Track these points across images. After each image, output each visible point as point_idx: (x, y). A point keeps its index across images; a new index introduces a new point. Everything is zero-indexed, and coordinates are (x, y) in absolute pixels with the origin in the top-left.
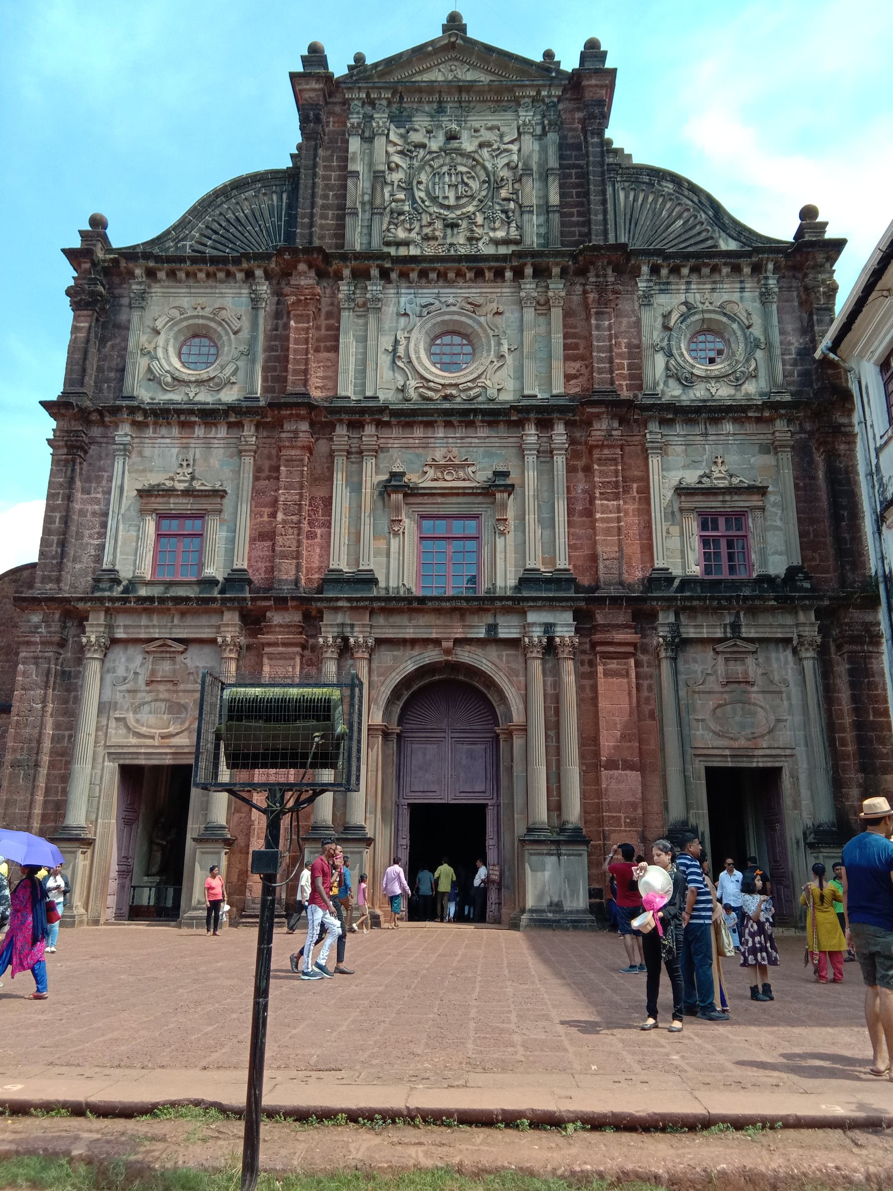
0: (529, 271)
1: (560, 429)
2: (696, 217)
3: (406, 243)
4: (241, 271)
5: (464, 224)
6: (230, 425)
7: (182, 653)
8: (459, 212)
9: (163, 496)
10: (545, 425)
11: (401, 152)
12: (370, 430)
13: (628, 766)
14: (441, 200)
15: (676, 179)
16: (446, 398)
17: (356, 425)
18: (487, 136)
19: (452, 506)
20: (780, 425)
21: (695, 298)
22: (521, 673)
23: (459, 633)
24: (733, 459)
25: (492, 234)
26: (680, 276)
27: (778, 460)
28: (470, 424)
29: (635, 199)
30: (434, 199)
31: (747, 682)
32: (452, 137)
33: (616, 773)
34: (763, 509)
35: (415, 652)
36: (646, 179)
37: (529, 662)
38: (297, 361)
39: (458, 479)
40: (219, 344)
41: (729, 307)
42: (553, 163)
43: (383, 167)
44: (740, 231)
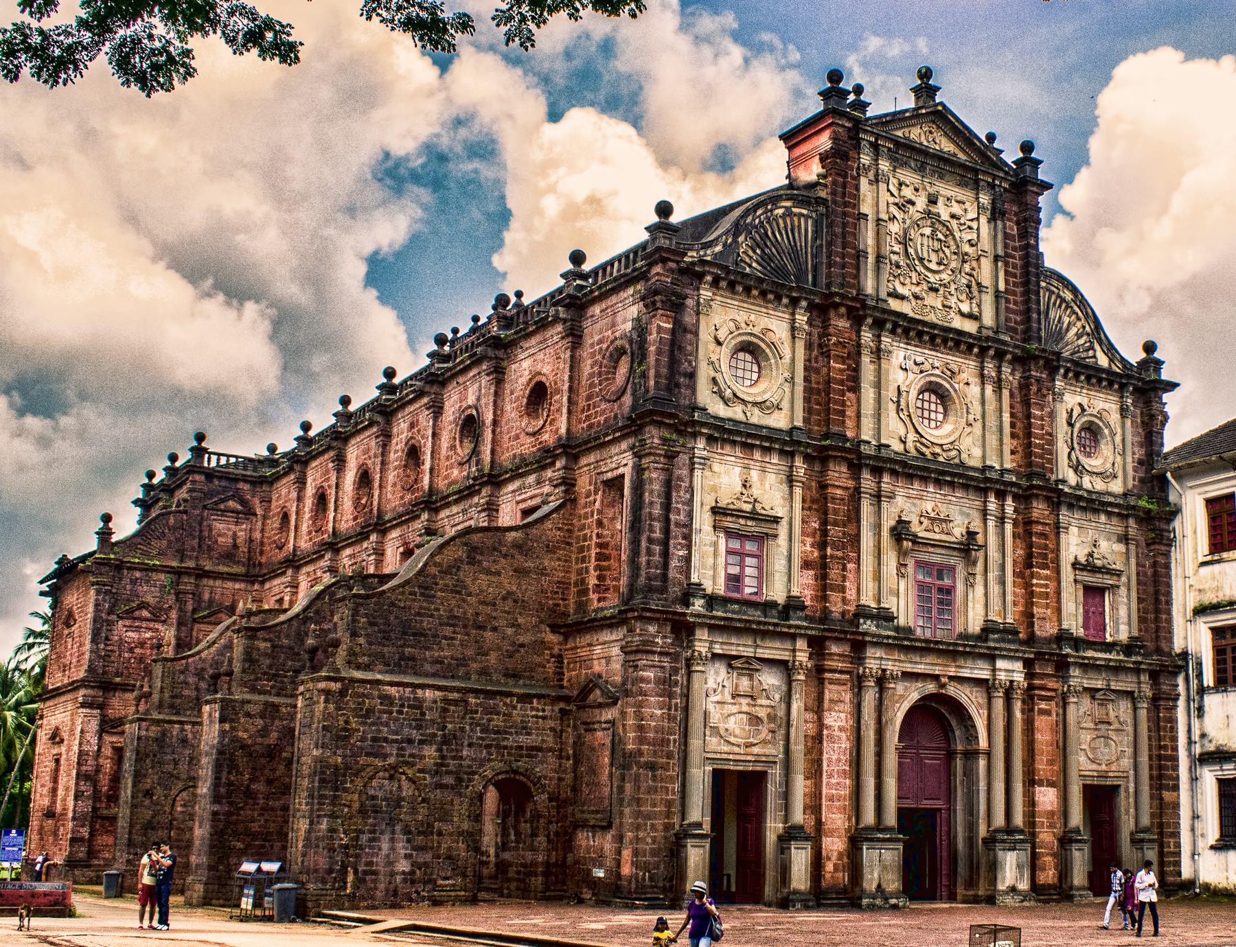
0: (992, 352)
2: (1084, 327)
4: (788, 296)
5: (942, 290)
6: (782, 452)
7: (757, 670)
8: (937, 277)
9: (732, 515)
10: (1001, 495)
11: (896, 204)
12: (886, 478)
13: (1051, 784)
14: (926, 262)
15: (1075, 291)
16: (933, 454)
17: (877, 472)
19: (936, 557)
20: (1131, 522)
21: (1085, 402)
22: (985, 706)
23: (952, 671)
24: (1104, 545)
25: (960, 304)
26: (1078, 380)
27: (1127, 549)
28: (952, 484)
30: (921, 260)
31: (1109, 723)
33: (1043, 789)
34: (1118, 587)
36: (1055, 283)
37: (994, 700)
38: (836, 402)
39: (942, 532)
41: (1104, 413)
43: (885, 217)
44: (1110, 350)
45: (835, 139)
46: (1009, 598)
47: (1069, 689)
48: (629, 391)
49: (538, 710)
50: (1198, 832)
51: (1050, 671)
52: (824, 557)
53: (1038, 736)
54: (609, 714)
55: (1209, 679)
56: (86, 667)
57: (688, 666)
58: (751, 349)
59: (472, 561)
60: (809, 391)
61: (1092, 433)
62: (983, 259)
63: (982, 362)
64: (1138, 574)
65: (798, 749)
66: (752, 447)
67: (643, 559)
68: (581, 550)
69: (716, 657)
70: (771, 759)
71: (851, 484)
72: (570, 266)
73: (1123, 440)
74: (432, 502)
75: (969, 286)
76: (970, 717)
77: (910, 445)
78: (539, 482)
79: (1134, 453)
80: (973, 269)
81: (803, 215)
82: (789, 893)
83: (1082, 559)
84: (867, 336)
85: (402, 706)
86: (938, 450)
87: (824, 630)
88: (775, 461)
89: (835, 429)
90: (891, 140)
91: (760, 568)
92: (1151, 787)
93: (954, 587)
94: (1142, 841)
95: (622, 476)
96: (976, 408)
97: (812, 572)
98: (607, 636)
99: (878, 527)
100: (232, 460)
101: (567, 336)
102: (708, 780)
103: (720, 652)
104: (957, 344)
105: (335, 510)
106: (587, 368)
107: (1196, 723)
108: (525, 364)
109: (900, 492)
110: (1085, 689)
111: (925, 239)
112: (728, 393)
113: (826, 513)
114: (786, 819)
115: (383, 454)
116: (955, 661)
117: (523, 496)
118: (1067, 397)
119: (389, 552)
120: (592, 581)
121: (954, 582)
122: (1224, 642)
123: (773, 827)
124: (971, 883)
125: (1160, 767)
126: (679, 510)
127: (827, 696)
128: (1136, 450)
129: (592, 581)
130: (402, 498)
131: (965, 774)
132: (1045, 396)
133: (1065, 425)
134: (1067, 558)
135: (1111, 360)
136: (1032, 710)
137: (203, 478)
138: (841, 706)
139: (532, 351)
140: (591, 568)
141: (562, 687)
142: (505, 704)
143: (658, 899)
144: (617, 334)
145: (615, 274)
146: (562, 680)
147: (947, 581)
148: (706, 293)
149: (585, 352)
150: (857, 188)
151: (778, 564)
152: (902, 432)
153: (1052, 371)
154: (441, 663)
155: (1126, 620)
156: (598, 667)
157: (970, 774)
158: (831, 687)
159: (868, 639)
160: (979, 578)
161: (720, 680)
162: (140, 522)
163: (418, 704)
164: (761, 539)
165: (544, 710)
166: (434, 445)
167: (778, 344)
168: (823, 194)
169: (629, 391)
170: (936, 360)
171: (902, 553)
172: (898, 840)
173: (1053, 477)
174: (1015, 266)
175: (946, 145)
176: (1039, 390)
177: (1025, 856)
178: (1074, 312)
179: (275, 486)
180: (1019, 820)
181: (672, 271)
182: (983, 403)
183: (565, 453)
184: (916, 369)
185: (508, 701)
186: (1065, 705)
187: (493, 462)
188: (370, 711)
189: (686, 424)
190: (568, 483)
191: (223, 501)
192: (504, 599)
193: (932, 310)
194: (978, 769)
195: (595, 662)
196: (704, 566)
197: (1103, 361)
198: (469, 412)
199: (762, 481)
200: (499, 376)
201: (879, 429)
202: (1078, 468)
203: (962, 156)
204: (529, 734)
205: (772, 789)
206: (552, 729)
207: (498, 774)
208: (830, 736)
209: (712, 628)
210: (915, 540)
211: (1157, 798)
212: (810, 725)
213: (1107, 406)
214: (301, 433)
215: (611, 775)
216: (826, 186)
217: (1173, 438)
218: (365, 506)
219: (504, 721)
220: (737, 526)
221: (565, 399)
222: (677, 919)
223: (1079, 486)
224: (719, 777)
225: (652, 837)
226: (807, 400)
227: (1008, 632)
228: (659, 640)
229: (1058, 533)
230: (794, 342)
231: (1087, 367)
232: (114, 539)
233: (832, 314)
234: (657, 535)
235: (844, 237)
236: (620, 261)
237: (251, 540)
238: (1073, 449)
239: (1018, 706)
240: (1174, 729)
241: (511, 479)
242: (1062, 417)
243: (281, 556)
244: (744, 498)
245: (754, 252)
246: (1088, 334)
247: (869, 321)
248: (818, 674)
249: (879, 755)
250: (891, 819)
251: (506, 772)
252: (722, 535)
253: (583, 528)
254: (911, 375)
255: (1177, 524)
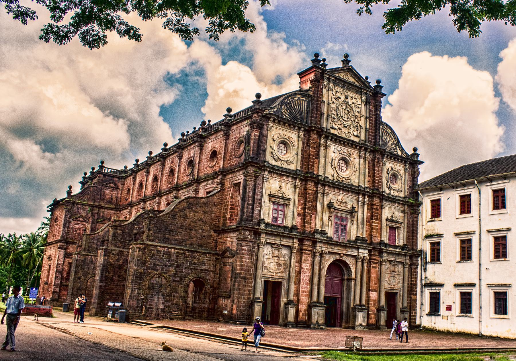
0: (363, 148)
1: (366, 197)
2: (394, 142)
3: (335, 129)
4: (297, 126)
5: (348, 128)
6: (293, 178)
7: (281, 248)
8: (347, 123)
9: (275, 197)
10: (364, 195)
11: (335, 98)
12: (326, 188)
13: (375, 291)
15: (391, 130)
16: (342, 181)
17: (324, 185)
18: (354, 101)
19: (341, 214)
20: (406, 206)
21: (393, 166)
22: (355, 264)
23: (345, 252)
26: (391, 159)
27: (404, 215)
28: (348, 191)
29: (383, 132)
30: (342, 117)
31: (395, 272)
32: (346, 98)
34: (400, 227)
35: (334, 256)
38: (311, 162)
39: (344, 206)
40: (288, 148)
42: (368, 116)
44: (402, 150)
45: (316, 76)
46: (365, 229)
47: (383, 260)
48: (244, 155)
49: (208, 258)
50: (423, 309)
51: (377, 254)
52: (305, 212)
53: (372, 275)
54: (232, 260)
55: (429, 259)
56: (61, 236)
57: (258, 246)
58: (284, 143)
59: (189, 208)
60: (303, 158)
61: (395, 177)
62: (362, 118)
63: (360, 151)
64: (407, 224)
65: (293, 275)
66: (283, 175)
67: (245, 210)
68: (225, 206)
69: (267, 243)
70: (284, 278)
71: (315, 189)
72: (227, 113)
73: (405, 180)
74: (177, 188)
75: (357, 126)
76: (350, 268)
77: (335, 177)
78: (213, 183)
79: (408, 184)
80: (359, 121)
81: (304, 100)
82: (287, 322)
83: (389, 218)
84: (323, 141)
85: (164, 254)
86: (344, 179)
87: (303, 236)
88: (290, 180)
89: (310, 171)
90: (334, 77)
91: (283, 215)
92: (408, 294)
93: (347, 225)
94: (404, 311)
95: (240, 182)
96: (357, 166)
97: (300, 217)
98: (232, 235)
99: (323, 203)
100: (113, 170)
101: (224, 136)
102: (263, 283)
103: (269, 242)
104: (352, 145)
105: (145, 189)
106: (230, 147)
107: (423, 273)
108: (210, 144)
109: (331, 192)
110: (388, 260)
111: (343, 110)
112: (276, 157)
113: (306, 198)
114: (288, 298)
115: (162, 171)
116: (346, 249)
117: (207, 187)
118: (387, 164)
119: (162, 203)
120: (228, 216)
121: (347, 223)
122: (434, 247)
123: (283, 300)
124: (347, 322)
125: (411, 287)
126: (258, 195)
127: (303, 258)
128: (409, 183)
129: (228, 216)
130: (167, 186)
131: (347, 286)
132: (380, 164)
133: (386, 173)
134: (384, 217)
135: (402, 153)
136: (370, 266)
137: (102, 176)
138: (308, 262)
139: (212, 140)
140: (228, 212)
141: (217, 250)
142: (198, 255)
143: (245, 322)
144: (241, 136)
145: (241, 116)
146: (217, 248)
147: (345, 223)
148: (270, 124)
149: (230, 141)
150: (322, 92)
151: (290, 214)
152: (332, 173)
153: (383, 155)
154: (177, 240)
155: (402, 238)
156: (229, 245)
157: (349, 286)
158: (305, 255)
159: (318, 240)
160: (355, 222)
161: (268, 251)
162: (81, 189)
163: (169, 254)
164: (284, 205)
165: (210, 258)
166: (179, 169)
167: (293, 142)
168: (311, 94)
169: (244, 155)
170: (345, 150)
171: (330, 213)
172: (324, 307)
173: (381, 190)
174: (372, 121)
175: (352, 80)
176: (378, 162)
177: (365, 314)
178: (391, 137)
179: (126, 180)
180: (364, 302)
181: (260, 116)
182: (359, 165)
183: (221, 174)
184: (338, 152)
185: (199, 254)
186: (381, 265)
187: (198, 175)
188: (153, 255)
189: (262, 167)
190: (222, 184)
191: (109, 184)
192: (199, 221)
193: (344, 133)
194: (351, 285)
195: (228, 243)
196: (265, 213)
197: (400, 153)
198: (191, 159)
199: (286, 186)
200: (201, 147)
201: (325, 171)
202: (389, 188)
203: (357, 84)
204: (205, 265)
205: (284, 288)
206: (212, 264)
207: (194, 278)
208: (304, 272)
209: (267, 234)
210: (335, 208)
211: (409, 297)
212: (297, 267)
213: (400, 168)
214: (136, 163)
215: (231, 280)
216: (312, 91)
217: (421, 180)
218: (155, 188)
219: (197, 261)
220: (277, 201)
221: (223, 156)
222: (250, 329)
223: (389, 194)
224: (266, 283)
225: (243, 301)
226: (302, 161)
227: (364, 240)
228: (249, 237)
229: (382, 209)
230: (299, 142)
231: (394, 155)
232: (72, 194)
233: (312, 133)
234: (250, 202)
235: (317, 108)
236: (243, 112)
237: (117, 197)
238: (388, 181)
239: (365, 265)
240: (416, 275)
241: (204, 182)
242: (385, 171)
243: (127, 203)
244: (280, 192)
245: (287, 111)
246: (395, 144)
247: (324, 136)
248: (301, 251)
249: (319, 278)
250: (322, 300)
251: (197, 277)
252: (272, 203)
253: (226, 199)
254: (336, 155)
255: (421, 208)
